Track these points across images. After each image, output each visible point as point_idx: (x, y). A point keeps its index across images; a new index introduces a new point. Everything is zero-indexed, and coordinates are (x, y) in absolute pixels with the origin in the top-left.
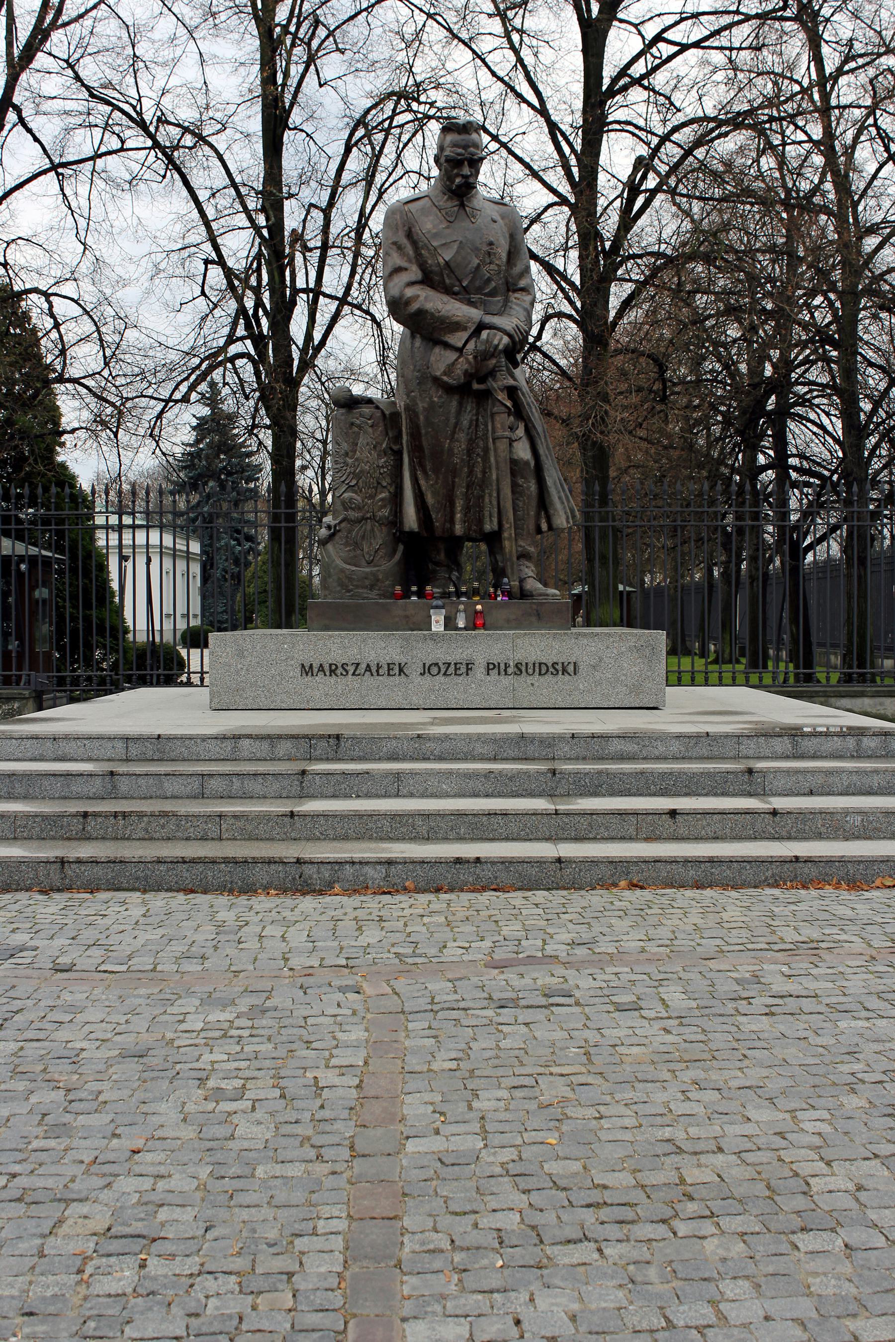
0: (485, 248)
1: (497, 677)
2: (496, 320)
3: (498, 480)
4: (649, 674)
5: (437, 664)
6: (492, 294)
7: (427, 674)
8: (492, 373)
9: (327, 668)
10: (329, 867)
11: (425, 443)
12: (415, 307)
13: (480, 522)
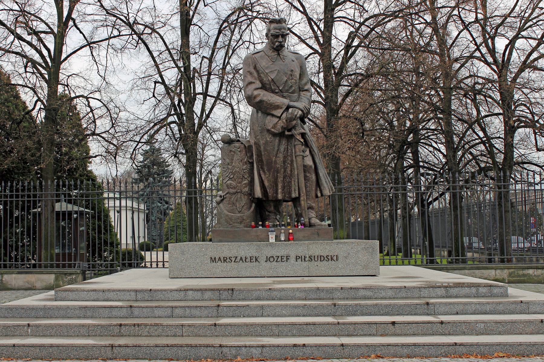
0: (289, 73)
1: (301, 262)
2: (295, 104)
3: (298, 174)
4: (372, 260)
5: (273, 257)
6: (293, 92)
8: (294, 127)
9: (222, 259)
10: (235, 348)
11: (264, 159)
12: (258, 99)
13: (290, 193)
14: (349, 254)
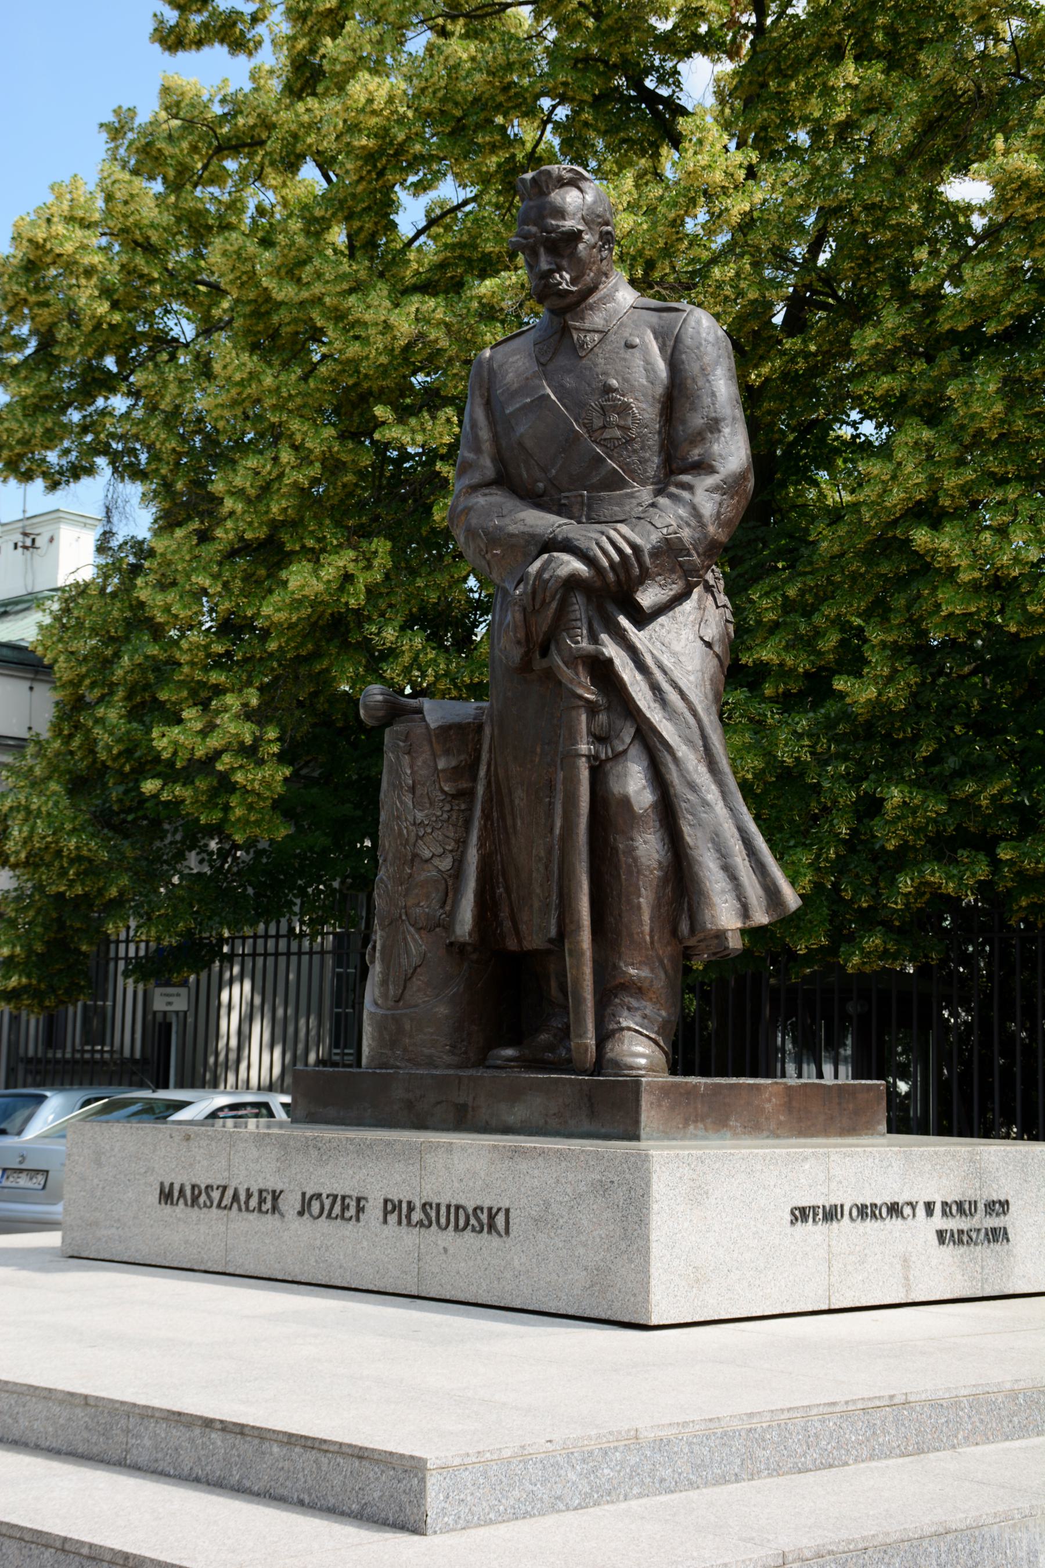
1: (397, 1228)
4: (623, 1246)
7: (307, 1215)
9: (188, 1193)
14: (547, 1205)
